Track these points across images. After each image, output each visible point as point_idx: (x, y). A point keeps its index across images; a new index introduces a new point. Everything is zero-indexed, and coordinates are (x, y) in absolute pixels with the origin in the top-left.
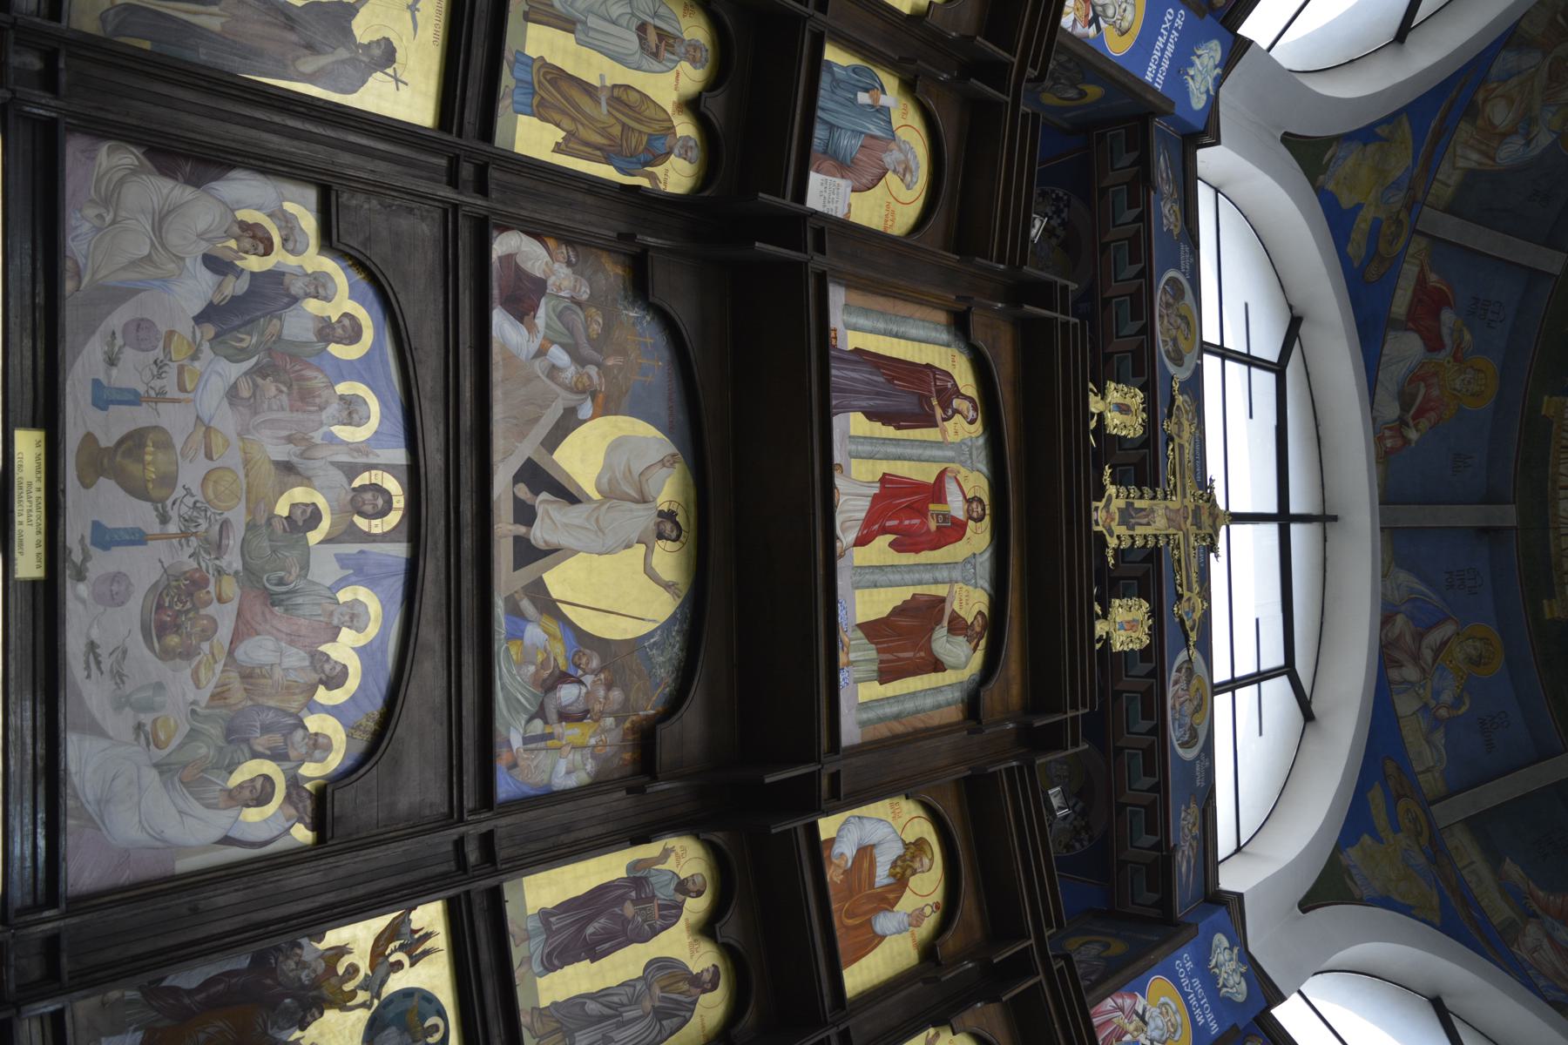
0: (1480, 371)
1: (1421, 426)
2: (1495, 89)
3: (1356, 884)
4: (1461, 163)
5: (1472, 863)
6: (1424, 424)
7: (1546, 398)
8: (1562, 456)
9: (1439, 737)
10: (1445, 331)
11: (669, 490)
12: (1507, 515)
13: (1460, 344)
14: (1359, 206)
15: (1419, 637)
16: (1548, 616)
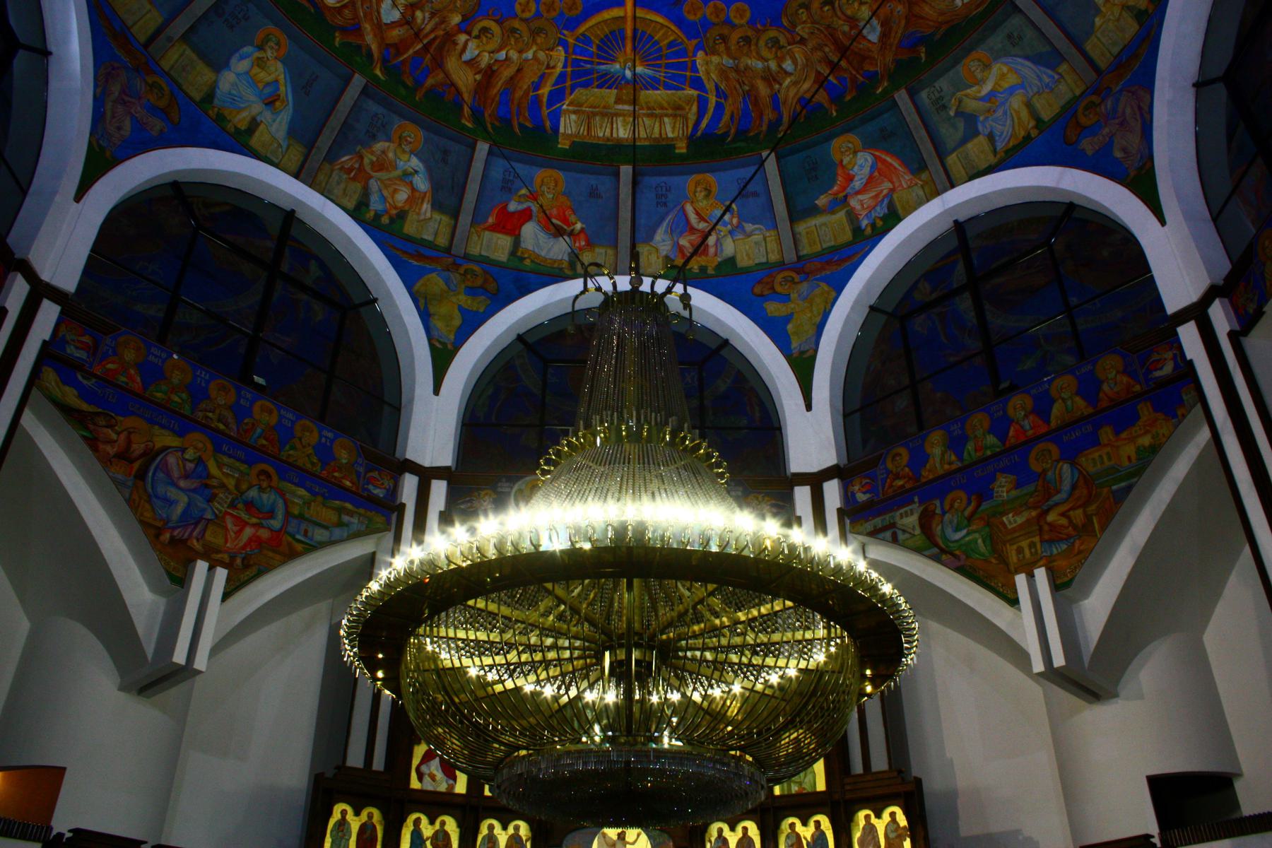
0: (542, 181)
1: (574, 221)
2: (390, 204)
3: (808, 351)
4: (428, 215)
5: (816, 226)
6: (572, 218)
7: (560, 146)
8: (593, 134)
9: (749, 227)
10: (521, 207)
11: (612, 833)
12: (626, 171)
13: (527, 196)
14: (461, 309)
15: (692, 230)
16: (684, 151)
